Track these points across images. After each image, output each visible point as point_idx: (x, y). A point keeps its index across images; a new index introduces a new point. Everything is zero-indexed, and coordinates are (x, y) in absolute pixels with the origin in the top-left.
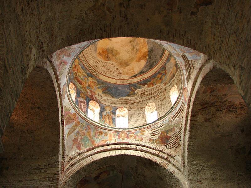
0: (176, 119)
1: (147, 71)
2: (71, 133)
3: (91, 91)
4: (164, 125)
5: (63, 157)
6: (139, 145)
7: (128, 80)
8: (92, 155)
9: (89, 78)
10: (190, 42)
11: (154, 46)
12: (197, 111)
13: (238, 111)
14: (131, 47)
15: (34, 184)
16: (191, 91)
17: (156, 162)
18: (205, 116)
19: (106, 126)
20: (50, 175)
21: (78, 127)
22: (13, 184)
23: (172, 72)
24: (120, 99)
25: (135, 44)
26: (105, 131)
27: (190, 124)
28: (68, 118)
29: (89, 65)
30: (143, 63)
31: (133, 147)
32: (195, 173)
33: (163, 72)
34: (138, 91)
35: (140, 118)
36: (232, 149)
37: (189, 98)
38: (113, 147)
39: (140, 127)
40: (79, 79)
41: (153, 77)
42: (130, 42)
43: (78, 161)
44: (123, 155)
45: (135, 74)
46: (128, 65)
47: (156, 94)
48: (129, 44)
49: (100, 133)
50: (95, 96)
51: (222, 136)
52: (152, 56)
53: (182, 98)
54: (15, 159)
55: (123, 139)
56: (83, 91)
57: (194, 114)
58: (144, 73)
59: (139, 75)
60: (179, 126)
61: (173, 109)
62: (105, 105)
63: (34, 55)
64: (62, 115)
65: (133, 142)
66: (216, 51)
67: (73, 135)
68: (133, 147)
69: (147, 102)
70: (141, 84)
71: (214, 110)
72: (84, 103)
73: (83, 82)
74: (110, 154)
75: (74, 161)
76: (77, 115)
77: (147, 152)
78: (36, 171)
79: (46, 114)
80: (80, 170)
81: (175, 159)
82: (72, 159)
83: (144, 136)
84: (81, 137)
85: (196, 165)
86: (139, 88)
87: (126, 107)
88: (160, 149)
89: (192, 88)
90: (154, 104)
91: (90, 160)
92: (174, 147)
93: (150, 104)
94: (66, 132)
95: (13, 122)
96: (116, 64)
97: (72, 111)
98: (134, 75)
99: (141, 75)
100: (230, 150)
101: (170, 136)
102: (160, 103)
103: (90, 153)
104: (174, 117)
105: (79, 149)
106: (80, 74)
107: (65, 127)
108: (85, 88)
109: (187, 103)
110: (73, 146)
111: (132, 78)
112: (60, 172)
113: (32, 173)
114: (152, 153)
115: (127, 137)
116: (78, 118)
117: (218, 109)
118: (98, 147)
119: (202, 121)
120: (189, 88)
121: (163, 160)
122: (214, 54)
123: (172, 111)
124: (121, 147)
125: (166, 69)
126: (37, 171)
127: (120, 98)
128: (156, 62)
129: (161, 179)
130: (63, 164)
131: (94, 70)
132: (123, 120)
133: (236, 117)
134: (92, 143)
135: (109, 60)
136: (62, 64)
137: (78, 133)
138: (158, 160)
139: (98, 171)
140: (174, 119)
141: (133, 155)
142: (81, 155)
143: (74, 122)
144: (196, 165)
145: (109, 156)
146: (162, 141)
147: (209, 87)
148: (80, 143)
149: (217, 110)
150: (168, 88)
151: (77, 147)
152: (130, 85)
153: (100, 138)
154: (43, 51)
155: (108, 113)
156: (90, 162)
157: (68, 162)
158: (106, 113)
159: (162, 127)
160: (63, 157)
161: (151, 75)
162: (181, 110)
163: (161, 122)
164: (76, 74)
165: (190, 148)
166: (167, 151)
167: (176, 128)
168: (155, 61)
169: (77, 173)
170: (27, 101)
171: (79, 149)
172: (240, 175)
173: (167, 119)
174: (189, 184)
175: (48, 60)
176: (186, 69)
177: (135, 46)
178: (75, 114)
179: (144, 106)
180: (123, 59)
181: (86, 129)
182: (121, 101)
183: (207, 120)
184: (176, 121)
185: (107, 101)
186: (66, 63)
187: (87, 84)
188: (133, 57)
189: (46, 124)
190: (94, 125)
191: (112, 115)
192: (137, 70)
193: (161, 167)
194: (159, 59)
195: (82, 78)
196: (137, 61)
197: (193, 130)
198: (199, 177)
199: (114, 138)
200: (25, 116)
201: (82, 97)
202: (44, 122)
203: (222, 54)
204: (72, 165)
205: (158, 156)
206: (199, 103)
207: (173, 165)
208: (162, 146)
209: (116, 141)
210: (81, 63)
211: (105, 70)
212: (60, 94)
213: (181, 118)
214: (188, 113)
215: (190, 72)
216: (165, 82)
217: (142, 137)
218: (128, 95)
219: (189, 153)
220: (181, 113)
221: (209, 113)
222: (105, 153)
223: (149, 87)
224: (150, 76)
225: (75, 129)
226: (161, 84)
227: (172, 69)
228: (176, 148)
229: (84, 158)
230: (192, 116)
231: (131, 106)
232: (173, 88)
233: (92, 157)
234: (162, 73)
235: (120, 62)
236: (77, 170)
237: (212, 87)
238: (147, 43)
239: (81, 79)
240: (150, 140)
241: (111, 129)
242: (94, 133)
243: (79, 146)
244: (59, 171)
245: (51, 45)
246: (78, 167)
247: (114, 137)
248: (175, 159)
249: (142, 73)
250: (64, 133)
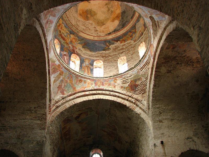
0: (143, 70)
1: (119, 30)
3: (73, 46)
4: (133, 75)
5: (50, 101)
6: (112, 91)
7: (104, 37)
8: (74, 99)
9: (71, 35)
10: (157, 5)
11: (126, 8)
12: (161, 64)
13: (194, 64)
14: (107, 9)
15: (27, 123)
16: (156, 47)
17: (126, 105)
18: (167, 68)
19: (85, 75)
20: (39, 115)
21: (62, 76)
22: (10, 122)
23: (140, 31)
24: (97, 53)
25: (110, 6)
26: (85, 79)
27: (155, 75)
28: (53, 68)
29: (71, 24)
30: (117, 23)
31: (108, 92)
32: (158, 115)
33: (133, 31)
34: (112, 47)
35: (114, 69)
36: (188, 96)
37: (155, 53)
38: (91, 92)
39: (113, 76)
40: (63, 35)
41: (124, 35)
42: (106, 4)
43: (62, 104)
44: (99, 99)
45: (109, 32)
46: (104, 24)
47: (127, 49)
48: (105, 6)
49: (81, 81)
50: (76, 50)
51: (181, 85)
52: (124, 17)
53: (149, 53)
54: (10, 102)
55: (99, 86)
56: (66, 46)
57: (158, 66)
58: (117, 31)
59: (113, 33)
60: (145, 76)
61: (141, 62)
62: (84, 58)
63: (25, 15)
64: (49, 66)
65: (107, 89)
66: (179, 13)
67: (58, 83)
68: (108, 92)
69: (119, 56)
70: (115, 41)
71: (175, 63)
72: (67, 56)
73: (66, 38)
74: (89, 98)
75: (59, 104)
76: (61, 66)
77: (119, 97)
78: (28, 112)
79: (36, 65)
80: (64, 111)
81: (141, 103)
82: (57, 102)
83: (116, 84)
85: (158, 108)
86: (113, 44)
87: (101, 60)
88: (129, 95)
89: (157, 45)
90: (125, 58)
91: (72, 103)
92: (141, 93)
93: (122, 58)
94: (52, 79)
95: (8, 71)
96: (94, 23)
97: (57, 63)
98: (109, 32)
99: (115, 33)
100: (187, 96)
101: (138, 84)
102: (130, 57)
103: (72, 97)
104: (141, 68)
105: (63, 94)
107: (51, 76)
108: (68, 43)
109: (153, 57)
111: (107, 36)
112: (48, 112)
113: (24, 114)
114: (123, 98)
115: (103, 85)
117: (178, 62)
118: (79, 92)
119: (164, 73)
120: (155, 44)
121: (132, 103)
122: (177, 16)
123: (140, 63)
124: (98, 92)
125: (136, 28)
126: (29, 112)
127: (98, 52)
128: (128, 22)
129: (130, 119)
130: (50, 106)
131: (75, 29)
132: (99, 70)
133: (193, 70)
134: (74, 90)
135: (88, 20)
136: (49, 23)
137: (62, 81)
138: (127, 104)
139: (79, 112)
140: (142, 70)
141: (107, 100)
142: (65, 99)
143: (59, 72)
144: (158, 108)
145: (88, 100)
146: (131, 88)
147: (172, 44)
148: (64, 89)
149: (178, 63)
150: (137, 44)
151: (61, 92)
152: (105, 41)
153: (80, 85)
154: (32, 11)
155: (87, 64)
157: (54, 105)
158: (86, 64)
159: (132, 76)
160: (50, 101)
161: (123, 33)
162: (147, 63)
163: (130, 72)
164: (60, 32)
165: (154, 94)
166: (135, 96)
167: (143, 78)
168: (127, 21)
169: (61, 114)
170: (19, 54)
171: (63, 94)
172: (194, 116)
173: (135, 70)
174: (152, 123)
175: (37, 19)
176: (153, 29)
177: (110, 8)
178: (59, 65)
179: (116, 59)
180: (100, 19)
181: (69, 78)
182: (98, 54)
183: (169, 72)
184: (143, 71)
185: (86, 54)
186: (52, 22)
187: (70, 40)
188: (109, 17)
189: (35, 74)
190: (76, 75)
191: (90, 66)
192: (112, 29)
193: (130, 109)
194: (130, 20)
195: (65, 35)
196: (111, 21)
197: (157, 80)
198: (160, 118)
199: (92, 85)
200: (18, 67)
201: (66, 51)
202: (34, 72)
203: (184, 16)
204: (57, 107)
205: (127, 100)
206: (163, 58)
207: (140, 108)
208: (131, 92)
209: (93, 88)
210: (64, 22)
211: (85, 28)
212: (47, 49)
213: (148, 69)
214: (153, 65)
215: (156, 31)
216: (134, 39)
217: (115, 85)
218: (104, 50)
219: (153, 98)
220: (148, 65)
221: (171, 66)
222: (84, 97)
223: (121, 43)
224: (123, 34)
225: (59, 78)
226: (131, 41)
227: (141, 28)
228: (142, 94)
229: (67, 101)
230: (156, 68)
231: (106, 59)
232: (141, 45)
233: (73, 101)
234: (132, 32)
235: (97, 21)
236: (61, 111)
237: (174, 43)
238: (121, 6)
239: (64, 35)
240: (122, 87)
241: (89, 77)
242: (76, 81)
244: (47, 112)
245: (39, 6)
246: (62, 109)
247: (92, 84)
248: (141, 103)
249: (115, 31)
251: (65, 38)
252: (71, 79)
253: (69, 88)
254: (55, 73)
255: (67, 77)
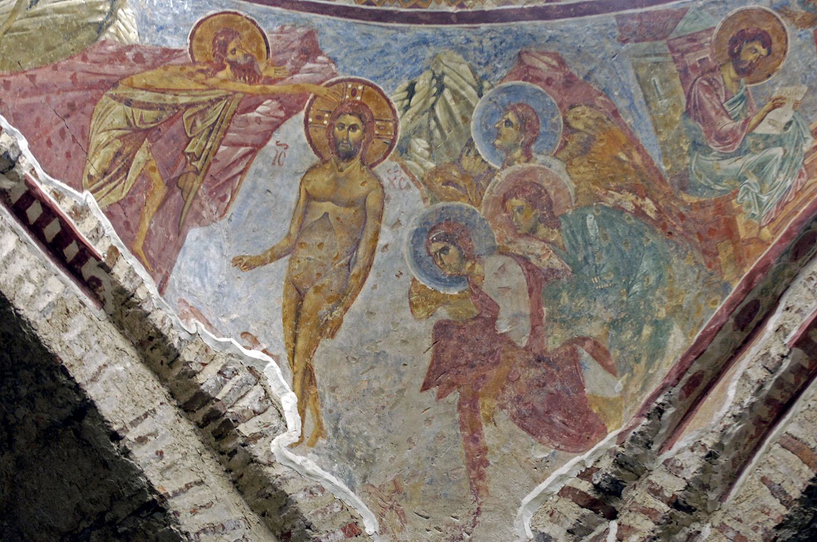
2: (342, 298)
21: (388, 170)
28: (136, 134)
49: (752, 52)
67: (389, 310)
84: (524, 260)
105: (580, 426)
107: (160, 264)
110: (474, 436)
116: (310, 50)
134: (710, 254)
137: (443, 236)
142: (637, 494)
143: (294, 131)
148: (554, 341)
151: (533, 422)
153: (784, 115)
156: (779, 510)
181: (527, 125)
225: (364, 218)
233: (792, 444)
242: (671, 102)
243: (554, 400)
250: (172, 356)
252: (583, 117)
253: (627, 272)
254: (222, 184)
255: (490, 135)
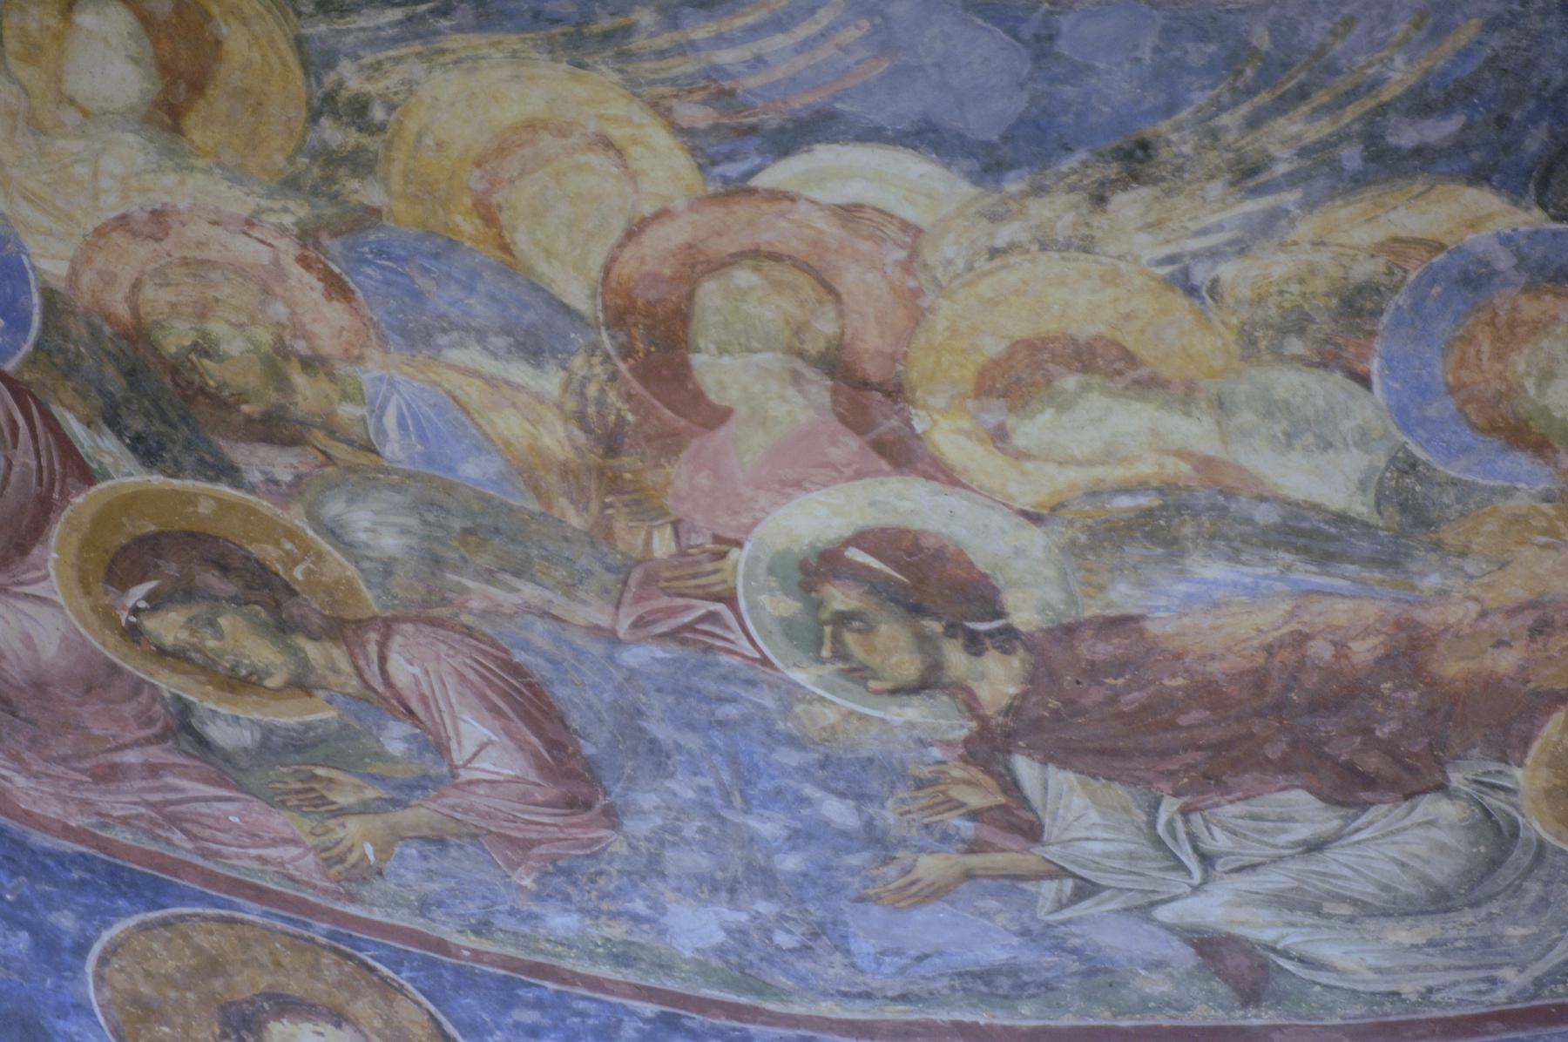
40: (1216, 610)
106: (1105, 439)
164: (935, 591)
195: (1331, 481)
239: (1311, 536)
251: (1410, 650)
